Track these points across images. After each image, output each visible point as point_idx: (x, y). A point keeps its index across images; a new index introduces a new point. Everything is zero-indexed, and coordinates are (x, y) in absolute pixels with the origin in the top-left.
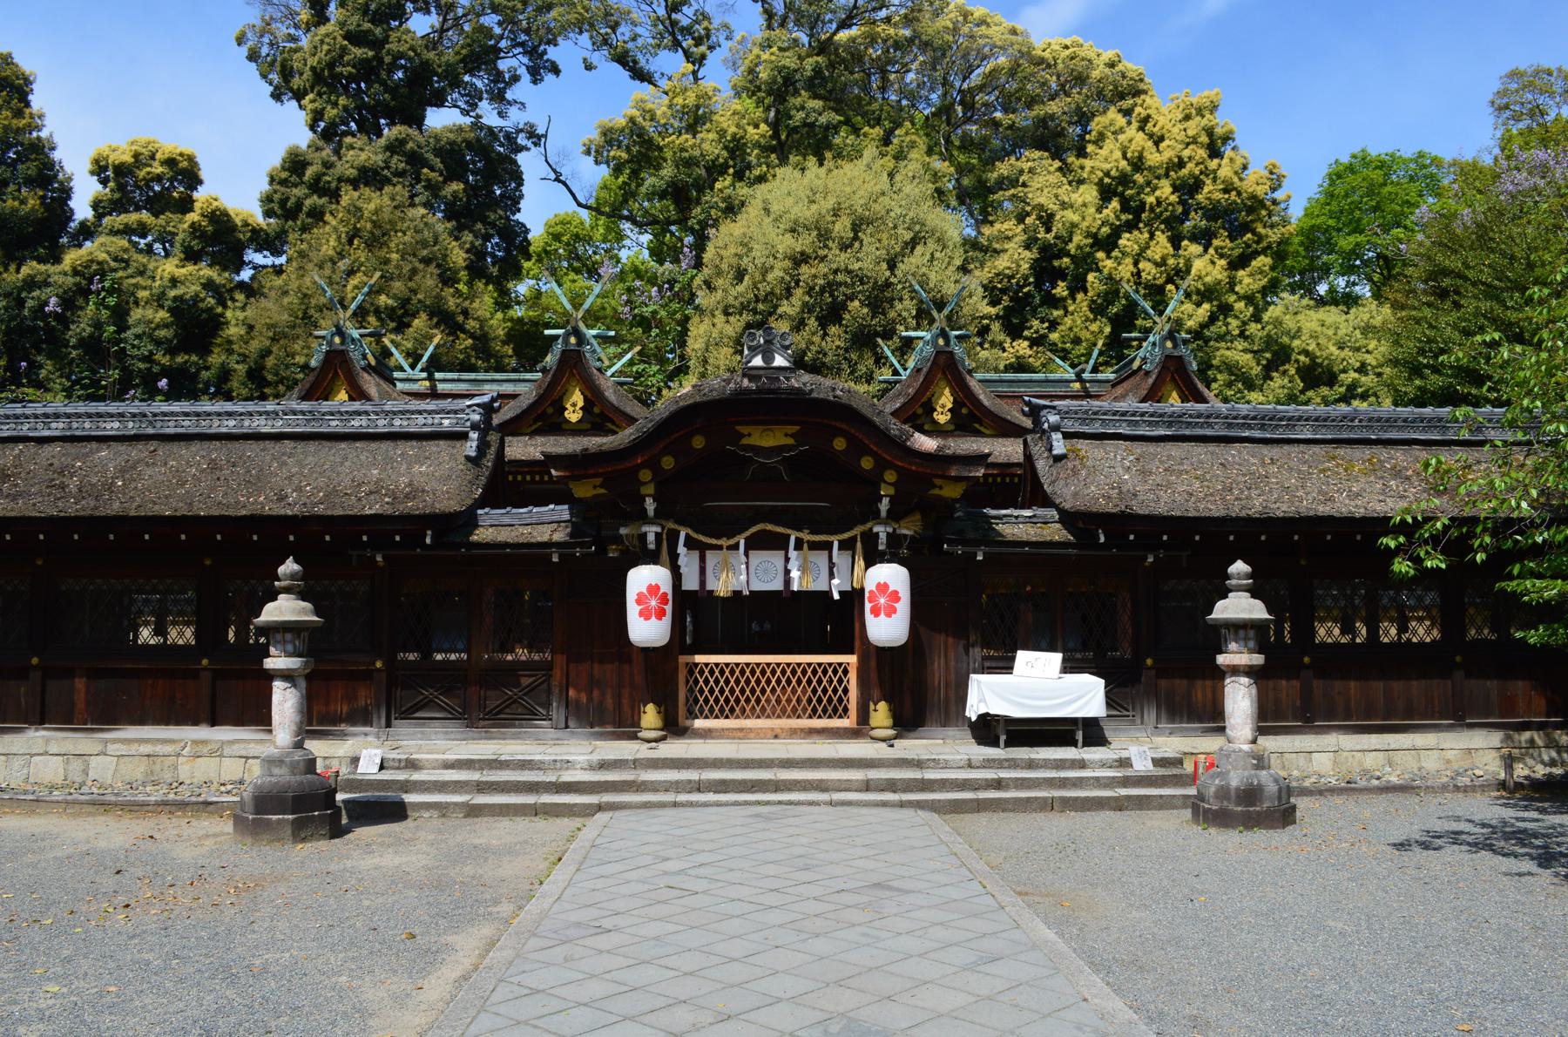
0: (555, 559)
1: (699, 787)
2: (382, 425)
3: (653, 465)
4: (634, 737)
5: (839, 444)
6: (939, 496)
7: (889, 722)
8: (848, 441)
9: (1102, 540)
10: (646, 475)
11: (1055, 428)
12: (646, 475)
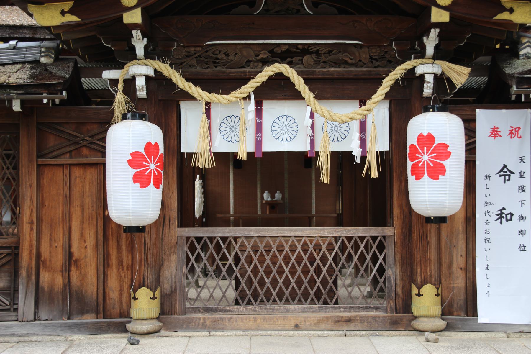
0: (16, 106)
6: (510, 23)
7: (438, 310)
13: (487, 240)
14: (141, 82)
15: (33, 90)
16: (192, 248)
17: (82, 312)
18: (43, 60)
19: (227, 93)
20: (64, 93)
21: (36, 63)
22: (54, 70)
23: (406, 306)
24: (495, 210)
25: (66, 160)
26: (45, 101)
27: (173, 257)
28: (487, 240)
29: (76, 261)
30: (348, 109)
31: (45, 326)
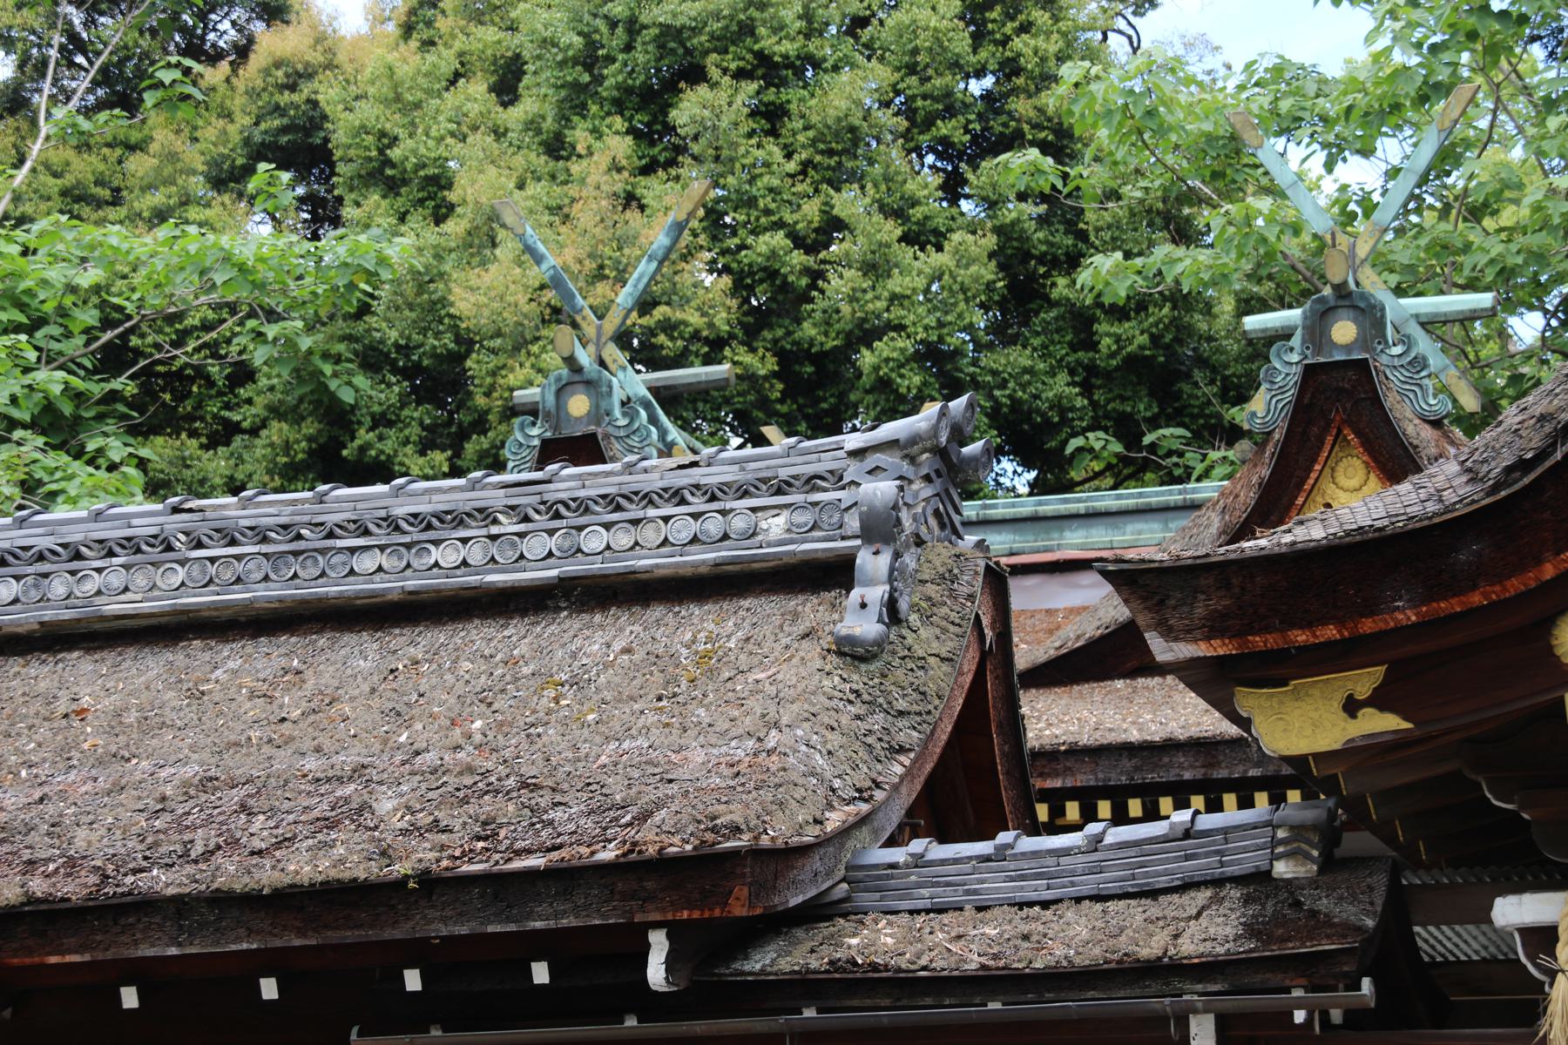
2: (538, 558)
15: (1257, 979)
18: (1282, 869)
20: (1366, 985)
21: (1258, 881)
22: (1324, 904)
26: (1299, 1016)
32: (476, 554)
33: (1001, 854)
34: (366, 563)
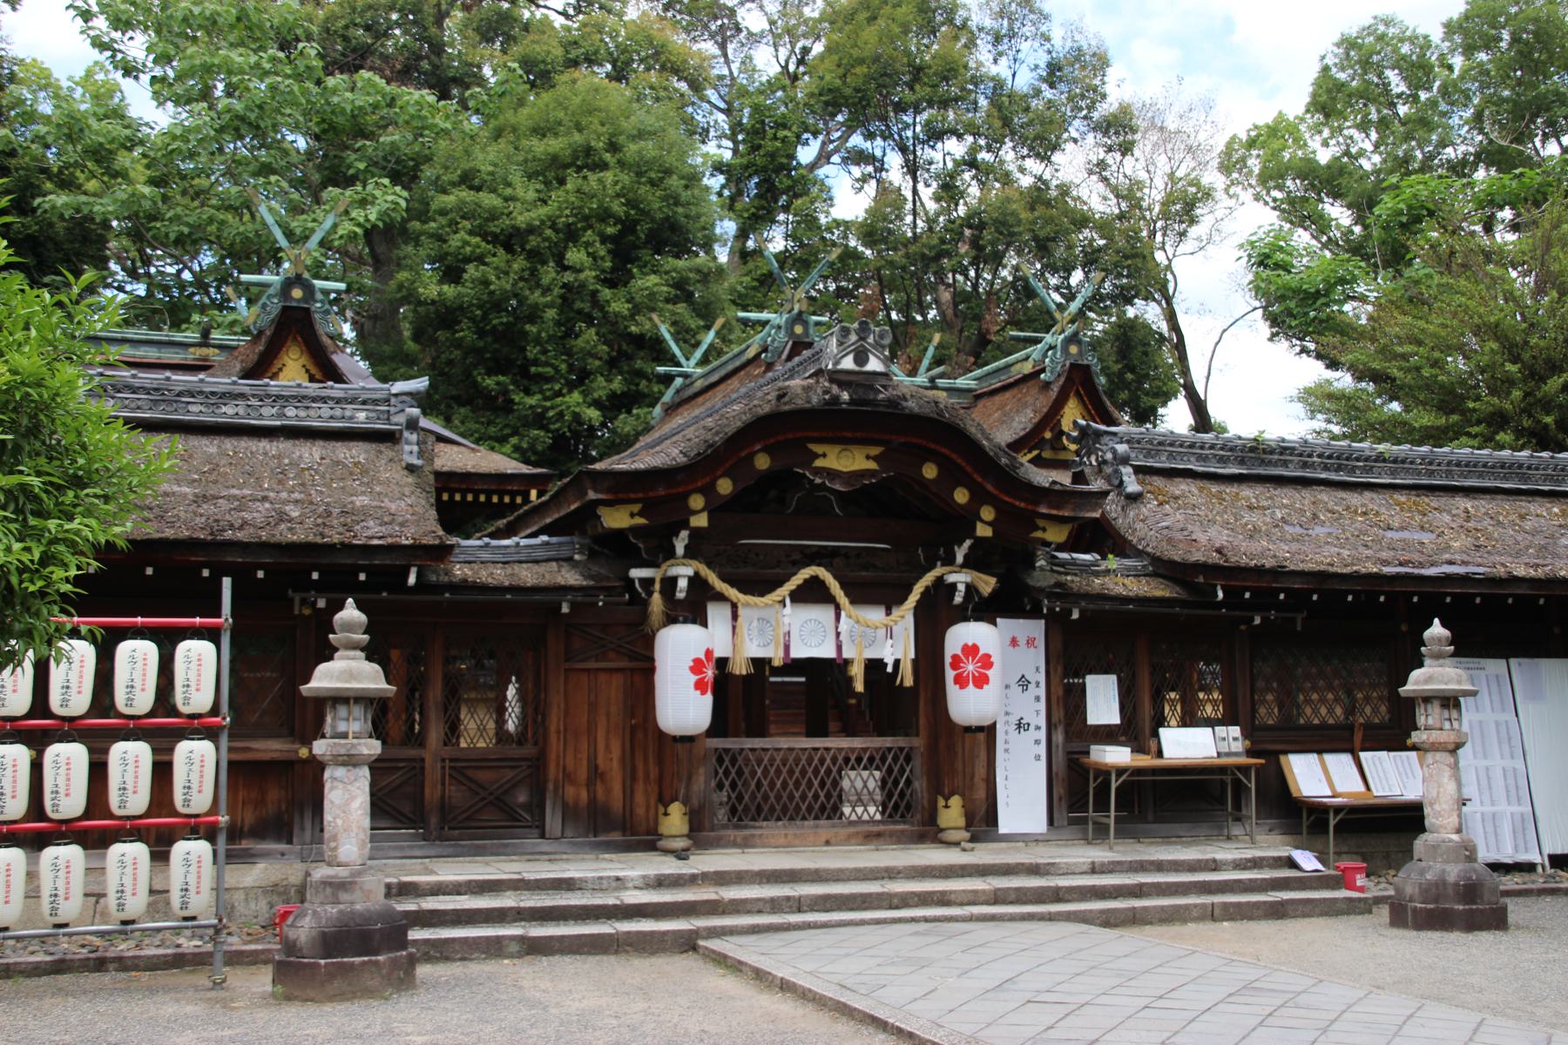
1: (798, 905)
3: (708, 491)
4: (651, 846)
5: (930, 471)
7: (962, 822)
8: (939, 465)
9: (1220, 595)
10: (697, 502)
11: (1125, 460)
12: (697, 502)
13: (1006, 750)
14: (683, 583)
16: (720, 761)
17: (609, 829)
19: (762, 595)
23: (931, 819)
24: (1014, 720)
25: (592, 665)
27: (702, 770)
28: (1006, 750)
29: (602, 774)
30: (875, 615)
31: (575, 844)
32: (241, 412)
33: (487, 545)
34: (193, 408)
